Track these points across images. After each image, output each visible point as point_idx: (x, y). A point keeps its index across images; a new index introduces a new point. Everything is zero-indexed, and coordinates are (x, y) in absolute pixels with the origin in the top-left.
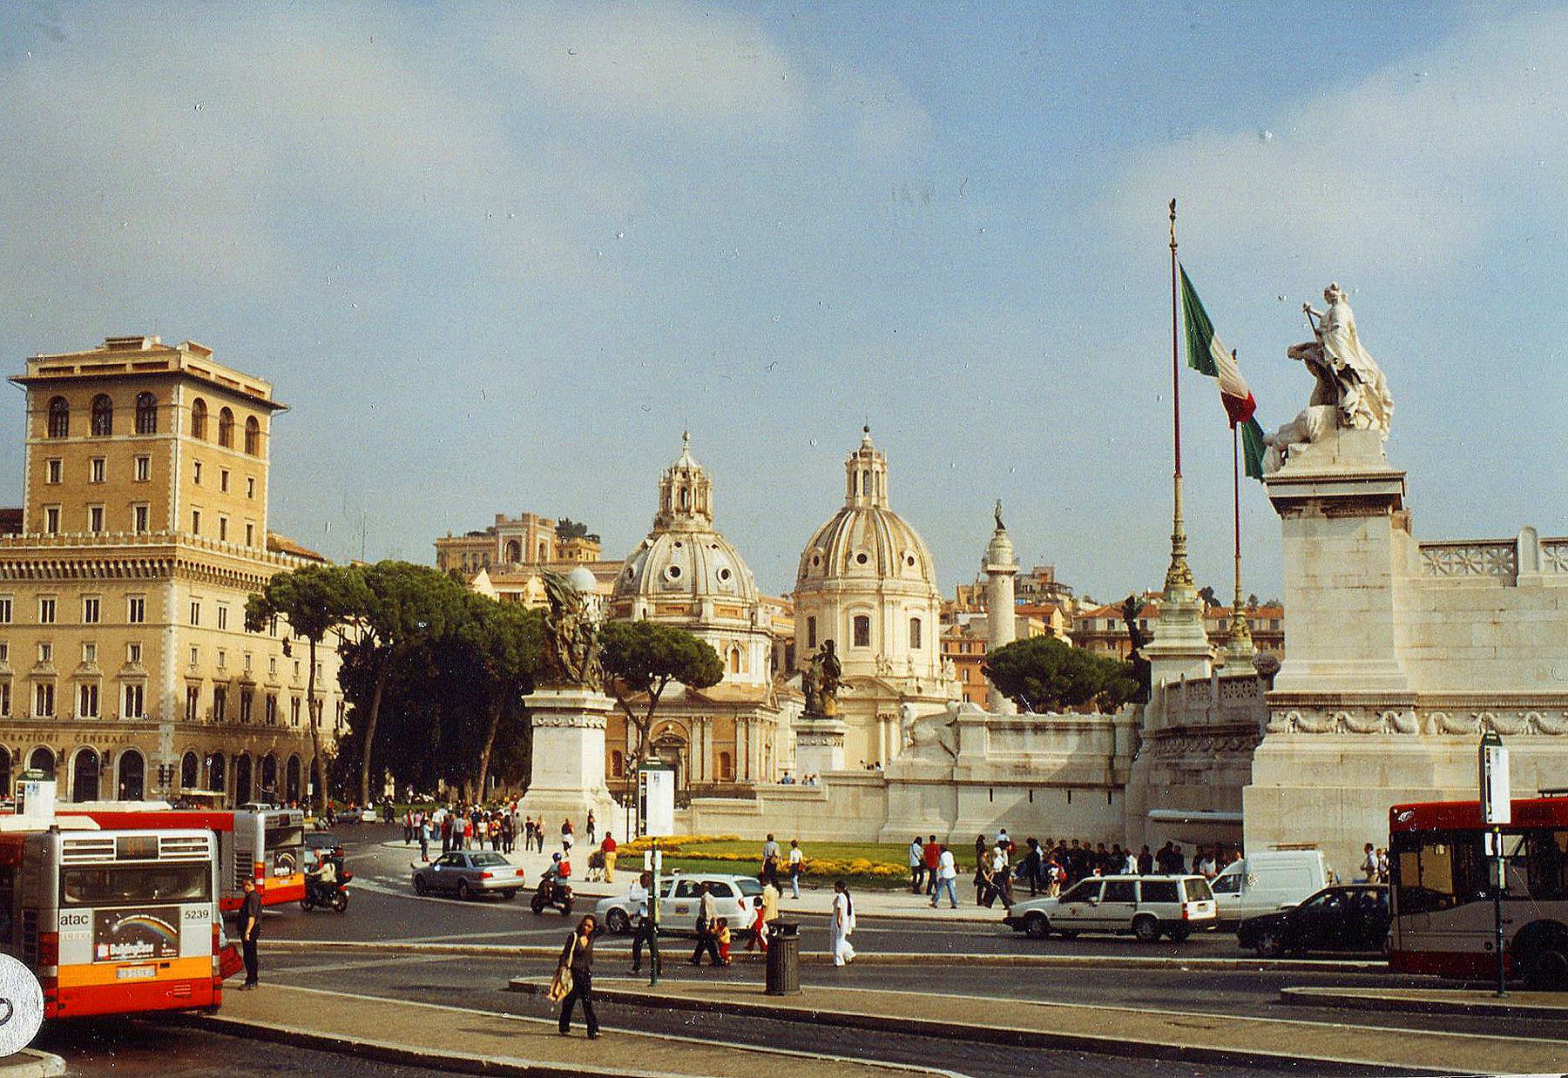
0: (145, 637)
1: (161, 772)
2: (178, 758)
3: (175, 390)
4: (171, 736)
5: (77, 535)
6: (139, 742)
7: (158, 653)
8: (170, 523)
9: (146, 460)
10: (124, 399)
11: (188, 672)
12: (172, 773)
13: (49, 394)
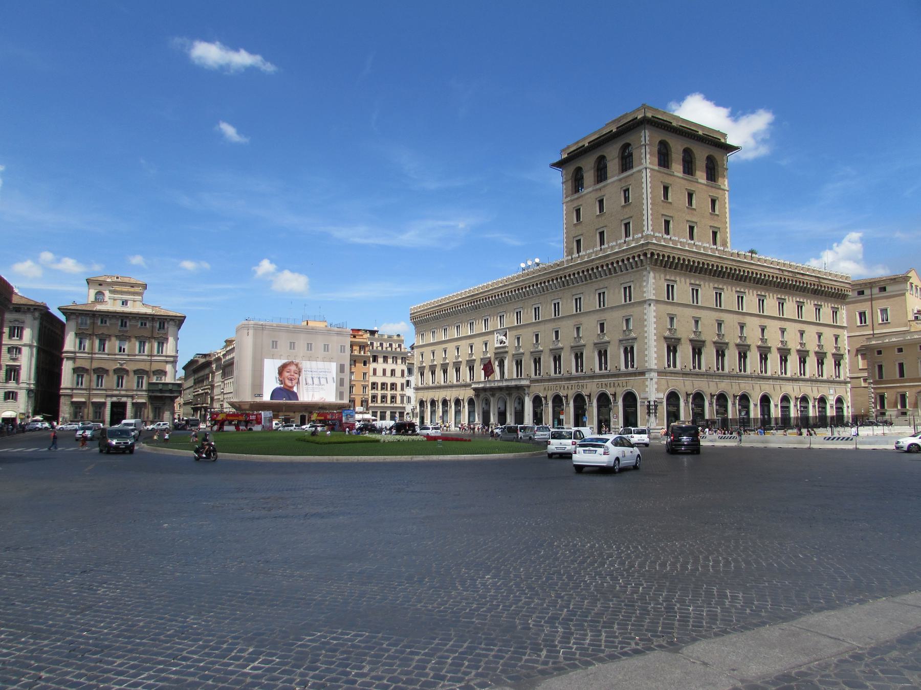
0: (634, 311)
1: (649, 406)
2: (663, 396)
3: (643, 134)
4: (655, 380)
5: (591, 252)
6: (633, 385)
7: (642, 321)
8: (645, 229)
9: (628, 190)
10: (612, 153)
11: (667, 334)
12: (656, 406)
13: (572, 168)
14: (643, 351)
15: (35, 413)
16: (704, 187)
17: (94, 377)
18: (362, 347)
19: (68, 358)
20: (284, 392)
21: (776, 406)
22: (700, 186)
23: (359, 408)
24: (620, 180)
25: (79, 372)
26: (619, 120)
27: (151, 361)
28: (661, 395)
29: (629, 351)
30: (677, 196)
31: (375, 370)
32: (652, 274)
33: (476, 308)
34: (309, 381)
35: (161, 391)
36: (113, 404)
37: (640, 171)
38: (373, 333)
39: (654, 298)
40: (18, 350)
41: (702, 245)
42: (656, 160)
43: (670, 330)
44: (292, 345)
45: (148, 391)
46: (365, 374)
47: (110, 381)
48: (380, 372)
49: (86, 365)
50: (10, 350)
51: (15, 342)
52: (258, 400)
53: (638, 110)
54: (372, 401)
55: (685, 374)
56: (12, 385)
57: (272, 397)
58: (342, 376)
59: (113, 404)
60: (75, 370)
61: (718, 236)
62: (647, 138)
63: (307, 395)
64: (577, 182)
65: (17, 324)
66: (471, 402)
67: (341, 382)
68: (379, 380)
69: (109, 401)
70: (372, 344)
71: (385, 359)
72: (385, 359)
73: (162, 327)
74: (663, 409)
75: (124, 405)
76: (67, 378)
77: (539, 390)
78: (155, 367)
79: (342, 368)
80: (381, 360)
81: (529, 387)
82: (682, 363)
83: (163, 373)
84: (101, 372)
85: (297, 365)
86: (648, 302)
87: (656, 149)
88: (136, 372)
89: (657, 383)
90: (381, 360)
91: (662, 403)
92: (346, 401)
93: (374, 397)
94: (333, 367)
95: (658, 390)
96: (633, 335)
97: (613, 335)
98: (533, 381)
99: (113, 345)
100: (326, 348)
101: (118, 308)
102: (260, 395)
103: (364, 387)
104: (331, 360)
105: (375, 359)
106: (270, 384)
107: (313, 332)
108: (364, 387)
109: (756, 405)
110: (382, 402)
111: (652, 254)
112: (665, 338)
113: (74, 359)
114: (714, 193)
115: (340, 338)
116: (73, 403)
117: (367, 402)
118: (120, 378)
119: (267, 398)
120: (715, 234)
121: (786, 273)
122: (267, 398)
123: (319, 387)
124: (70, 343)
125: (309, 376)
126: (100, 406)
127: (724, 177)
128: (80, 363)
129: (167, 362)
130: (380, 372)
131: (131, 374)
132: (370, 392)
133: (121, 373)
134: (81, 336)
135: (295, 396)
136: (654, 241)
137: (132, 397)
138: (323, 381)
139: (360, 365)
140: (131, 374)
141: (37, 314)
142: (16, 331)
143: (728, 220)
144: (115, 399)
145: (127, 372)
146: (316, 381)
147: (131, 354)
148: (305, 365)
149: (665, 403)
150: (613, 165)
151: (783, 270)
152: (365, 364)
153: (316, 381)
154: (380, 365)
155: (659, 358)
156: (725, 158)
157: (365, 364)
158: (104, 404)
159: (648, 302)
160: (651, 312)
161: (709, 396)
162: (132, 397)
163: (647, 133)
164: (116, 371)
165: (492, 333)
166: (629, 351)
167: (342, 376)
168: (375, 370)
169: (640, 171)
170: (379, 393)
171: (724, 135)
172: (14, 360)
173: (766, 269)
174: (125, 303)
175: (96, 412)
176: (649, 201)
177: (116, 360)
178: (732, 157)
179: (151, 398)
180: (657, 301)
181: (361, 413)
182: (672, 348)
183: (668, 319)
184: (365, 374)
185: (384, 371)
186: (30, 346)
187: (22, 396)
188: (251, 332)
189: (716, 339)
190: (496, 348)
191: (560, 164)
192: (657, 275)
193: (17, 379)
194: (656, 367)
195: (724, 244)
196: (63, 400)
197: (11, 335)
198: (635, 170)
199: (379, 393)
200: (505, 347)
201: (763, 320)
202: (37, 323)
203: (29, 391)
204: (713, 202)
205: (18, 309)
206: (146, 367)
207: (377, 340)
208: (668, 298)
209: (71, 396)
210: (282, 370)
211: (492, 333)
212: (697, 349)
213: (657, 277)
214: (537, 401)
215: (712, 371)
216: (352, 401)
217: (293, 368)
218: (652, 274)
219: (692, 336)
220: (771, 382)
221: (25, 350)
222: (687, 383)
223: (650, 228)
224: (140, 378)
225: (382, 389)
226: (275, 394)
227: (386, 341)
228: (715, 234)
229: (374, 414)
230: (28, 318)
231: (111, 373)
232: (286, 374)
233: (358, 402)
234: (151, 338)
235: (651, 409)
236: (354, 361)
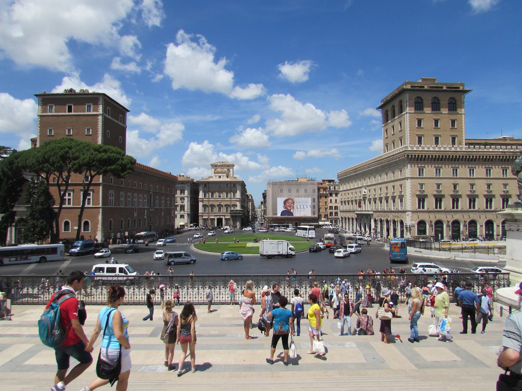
6: (401, 217)
11: (418, 193)
12: (410, 228)
14: (405, 201)
15: (191, 223)
16: (447, 115)
17: (210, 208)
18: (325, 189)
19: (201, 201)
20: (287, 212)
21: (498, 226)
22: (443, 115)
23: (323, 219)
24: (398, 118)
25: (204, 206)
26: (398, 88)
27: (231, 201)
28: (414, 223)
29: (401, 201)
30: (428, 123)
31: (331, 200)
32: (409, 165)
33: (357, 175)
34: (299, 207)
35: (235, 213)
36: (218, 219)
37: (404, 114)
38: (330, 181)
39: (410, 176)
41: (445, 147)
42: (413, 108)
43: (420, 191)
44: (290, 191)
45: (230, 213)
46: (326, 202)
47: (216, 210)
48: (333, 201)
49: (206, 203)
50: (181, 199)
51: (182, 196)
52: (275, 216)
53: (403, 85)
54: (330, 215)
55: (429, 212)
56: (182, 212)
57: (281, 215)
58: (314, 204)
59: (218, 219)
60: (204, 206)
61: (456, 139)
62: (407, 98)
63: (297, 213)
64: (386, 119)
65: (182, 189)
66: (356, 220)
67: (314, 207)
68: (334, 205)
69: (216, 218)
70: (330, 187)
71: (336, 195)
72: (336, 195)
73: (234, 186)
74: (415, 230)
75: (222, 219)
76: (201, 209)
77: (375, 216)
78: (233, 203)
79: (314, 200)
80: (334, 195)
81: (373, 214)
82: (427, 206)
83: (236, 206)
84: (212, 206)
85: (292, 200)
86: (407, 178)
87: (413, 101)
88: (226, 205)
89: (411, 217)
90: (334, 195)
91: (414, 226)
92: (316, 216)
93: (331, 214)
94: (310, 200)
95: (411, 220)
96: (403, 194)
97: (397, 194)
98: (374, 212)
99: (216, 195)
100: (306, 191)
101: (217, 179)
102: (276, 214)
103: (326, 209)
104: (308, 197)
105: (331, 195)
106: (280, 209)
107: (301, 184)
108: (326, 209)
109: (481, 226)
110: (335, 215)
111: (408, 156)
112: (417, 195)
113: (203, 201)
114: (453, 117)
115: (312, 186)
116: (203, 219)
117: (327, 215)
118: (220, 208)
119: (279, 215)
120: (453, 139)
121: (508, 153)
122: (279, 215)
123: (303, 208)
124: (201, 195)
125: (298, 204)
127: (461, 107)
128: (205, 203)
129: (237, 201)
130: (333, 201)
131: (224, 206)
132: (329, 211)
133: (220, 206)
134: (205, 193)
135: (292, 214)
136: (410, 149)
137: (224, 216)
138: (305, 207)
139: (323, 200)
140: (224, 206)
141: (189, 184)
142: (182, 192)
143: (463, 130)
144: (218, 217)
145: (222, 206)
146: (302, 207)
147: (224, 198)
148: (296, 199)
149: (416, 226)
150: (397, 109)
151: (504, 152)
152: (326, 198)
153: (302, 207)
154: (334, 198)
155: (413, 204)
156: (463, 96)
157: (326, 198)
158: (214, 219)
159: (407, 178)
160: (408, 183)
161: (447, 223)
162: (224, 216)
163: (407, 95)
164: (218, 205)
165: (361, 187)
166: (401, 201)
167: (314, 204)
168: (331, 200)
169: (404, 114)
170: (334, 211)
171: (463, 85)
172: (183, 202)
173: (496, 153)
174: (220, 177)
175: (211, 223)
176: (408, 129)
177: (218, 201)
178: (467, 96)
179: (232, 217)
180: (412, 178)
181: (324, 221)
182: (421, 199)
183: (419, 186)
184: (326, 202)
185: (336, 200)
186: (187, 197)
187: (186, 216)
188: (271, 186)
189: (452, 193)
190: (364, 195)
191: (381, 107)
192: (413, 166)
193: (184, 210)
194: (411, 209)
195: (460, 143)
196: (200, 218)
197: (181, 193)
198: (403, 113)
199: (334, 211)
200: (365, 195)
201: (489, 180)
202: (189, 188)
203: (188, 214)
204: (453, 122)
205: (182, 183)
206: (229, 203)
207: (332, 185)
208: (420, 175)
209: (203, 216)
210: (285, 202)
211: (361, 187)
212: (439, 199)
213: (413, 166)
214: (375, 221)
215: (448, 209)
216: (320, 216)
217: (290, 201)
218: (409, 165)
219: (435, 193)
220: (494, 213)
221: (186, 198)
222: (431, 216)
223: (409, 142)
224: (227, 208)
225: (335, 209)
226: (283, 213)
227: (337, 185)
228: (453, 139)
229: (331, 222)
230: (186, 186)
231: (216, 206)
232: (287, 204)
233: (323, 215)
234: (231, 191)
235: (409, 229)
236: (320, 196)
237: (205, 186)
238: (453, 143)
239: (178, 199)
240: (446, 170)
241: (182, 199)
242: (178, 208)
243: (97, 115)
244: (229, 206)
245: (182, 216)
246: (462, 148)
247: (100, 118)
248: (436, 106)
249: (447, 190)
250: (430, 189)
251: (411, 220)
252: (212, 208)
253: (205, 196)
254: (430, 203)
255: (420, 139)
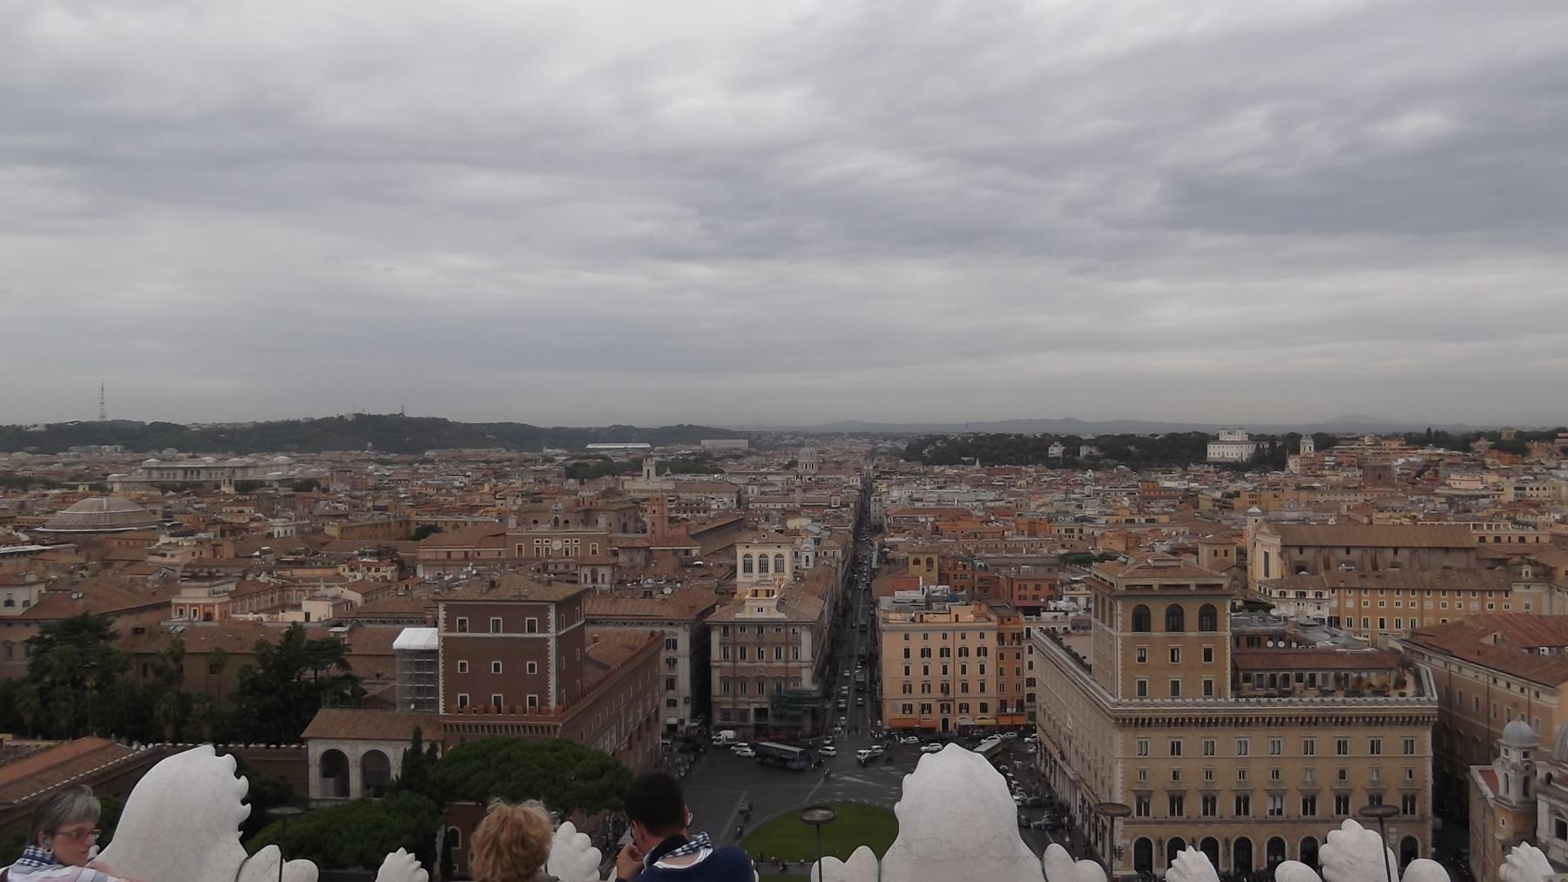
31: (1031, 664)
36: (756, 710)
40: (675, 661)
50: (668, 661)
51: (670, 653)
59: (756, 710)
84: (744, 681)
95: (1124, 837)
120: (1208, 684)
124: (716, 652)
126: (744, 713)
168: (1031, 664)
177: (755, 668)
212: (1176, 801)
237: (726, 628)
238: (1208, 691)
239: (662, 662)
240: (1192, 740)
241: (672, 662)
242: (663, 683)
243: (546, 640)
244: (787, 679)
245: (672, 703)
246: (1226, 702)
247: (552, 644)
248: (1175, 621)
249: (1193, 783)
250: (1160, 781)
251: (1124, 837)
252: (744, 686)
253: (726, 656)
254: (1160, 806)
255: (1142, 685)
